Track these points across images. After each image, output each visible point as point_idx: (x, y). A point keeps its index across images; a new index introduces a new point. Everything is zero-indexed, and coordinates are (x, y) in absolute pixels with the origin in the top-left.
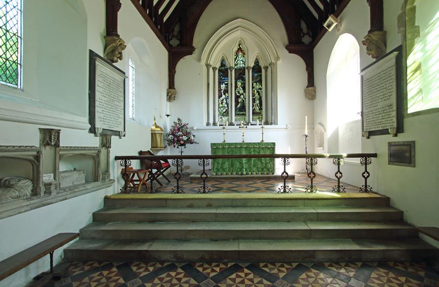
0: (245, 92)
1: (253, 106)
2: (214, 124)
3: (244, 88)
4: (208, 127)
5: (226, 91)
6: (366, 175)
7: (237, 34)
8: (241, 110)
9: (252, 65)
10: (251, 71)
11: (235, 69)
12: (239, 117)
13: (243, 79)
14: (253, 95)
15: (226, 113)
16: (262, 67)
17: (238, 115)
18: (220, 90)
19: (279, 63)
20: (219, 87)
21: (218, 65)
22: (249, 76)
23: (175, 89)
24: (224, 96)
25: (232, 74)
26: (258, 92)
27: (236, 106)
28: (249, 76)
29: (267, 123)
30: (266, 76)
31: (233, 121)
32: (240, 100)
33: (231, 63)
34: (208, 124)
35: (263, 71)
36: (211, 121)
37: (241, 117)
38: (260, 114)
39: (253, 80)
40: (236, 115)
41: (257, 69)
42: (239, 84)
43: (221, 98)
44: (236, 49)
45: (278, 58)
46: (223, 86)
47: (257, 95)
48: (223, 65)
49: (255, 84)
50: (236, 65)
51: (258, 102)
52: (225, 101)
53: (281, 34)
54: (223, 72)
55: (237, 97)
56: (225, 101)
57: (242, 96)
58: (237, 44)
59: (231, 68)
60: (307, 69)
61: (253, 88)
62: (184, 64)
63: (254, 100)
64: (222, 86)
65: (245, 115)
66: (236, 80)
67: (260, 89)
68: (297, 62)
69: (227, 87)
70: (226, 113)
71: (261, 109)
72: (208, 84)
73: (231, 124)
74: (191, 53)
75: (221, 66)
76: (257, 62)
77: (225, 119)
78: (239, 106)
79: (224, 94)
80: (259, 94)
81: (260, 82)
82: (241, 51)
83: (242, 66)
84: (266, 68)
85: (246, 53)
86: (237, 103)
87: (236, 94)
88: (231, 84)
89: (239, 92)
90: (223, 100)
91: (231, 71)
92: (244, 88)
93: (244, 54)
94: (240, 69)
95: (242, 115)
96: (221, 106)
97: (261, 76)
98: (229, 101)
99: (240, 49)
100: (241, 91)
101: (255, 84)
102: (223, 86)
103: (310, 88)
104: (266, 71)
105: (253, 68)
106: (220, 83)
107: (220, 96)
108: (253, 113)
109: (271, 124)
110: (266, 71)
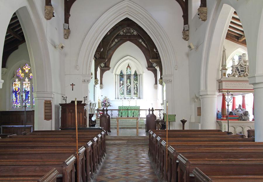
0: (130, 85)
1: (134, 90)
2: (118, 98)
3: (130, 83)
4: (115, 100)
5: (123, 84)
6: (160, 115)
7: (128, 62)
8: (129, 92)
9: (133, 73)
10: (133, 76)
11: (127, 75)
12: (128, 95)
13: (130, 79)
14: (134, 85)
15: (123, 94)
16: (138, 74)
17: (128, 94)
18: (120, 84)
19: (144, 74)
20: (120, 82)
21: (119, 73)
22: (132, 78)
23: (102, 84)
24: (122, 86)
25: (125, 77)
26: (136, 85)
27: (127, 91)
28: (132, 78)
29: (139, 98)
30: (139, 79)
31: (126, 97)
32: (128, 88)
33: (125, 73)
34: (116, 98)
35: (138, 76)
36: (117, 97)
37: (129, 95)
38: (137, 94)
39: (134, 79)
40: (127, 94)
41: (136, 75)
42: (128, 81)
43: (121, 87)
44: (127, 66)
45: (143, 72)
46: (121, 82)
47: (135, 86)
48: (121, 73)
49: (135, 81)
50: (127, 73)
51: (136, 89)
52: (122, 88)
53: (144, 62)
54: (122, 75)
55: (127, 87)
56: (122, 88)
57: (129, 86)
58: (128, 64)
59: (125, 75)
60: (155, 76)
61: (134, 83)
62: (106, 74)
63: (134, 88)
64: (121, 82)
65: (131, 94)
66: (127, 79)
67: (137, 83)
68: (151, 74)
69: (123, 82)
70: (123, 94)
71: (137, 92)
72: (116, 82)
73: (125, 99)
74: (109, 70)
75: (121, 74)
76: (136, 72)
77: (123, 96)
78: (128, 90)
79: (122, 85)
80: (136, 86)
81: (137, 80)
82: (129, 67)
83: (129, 73)
84: (139, 75)
85: (131, 68)
86: (127, 89)
87: (127, 85)
88: (125, 82)
89: (128, 85)
90: (121, 88)
91: (125, 76)
92: (130, 83)
93: (130, 68)
94: (129, 75)
95: (129, 94)
96: (120, 90)
97: (137, 78)
98: (124, 88)
99: (129, 66)
100: (129, 84)
101: (135, 81)
102: (121, 82)
103: (156, 85)
104: (139, 76)
105: (134, 75)
106: (120, 80)
107: (120, 86)
108: (134, 94)
109: (141, 99)
110: (139, 76)
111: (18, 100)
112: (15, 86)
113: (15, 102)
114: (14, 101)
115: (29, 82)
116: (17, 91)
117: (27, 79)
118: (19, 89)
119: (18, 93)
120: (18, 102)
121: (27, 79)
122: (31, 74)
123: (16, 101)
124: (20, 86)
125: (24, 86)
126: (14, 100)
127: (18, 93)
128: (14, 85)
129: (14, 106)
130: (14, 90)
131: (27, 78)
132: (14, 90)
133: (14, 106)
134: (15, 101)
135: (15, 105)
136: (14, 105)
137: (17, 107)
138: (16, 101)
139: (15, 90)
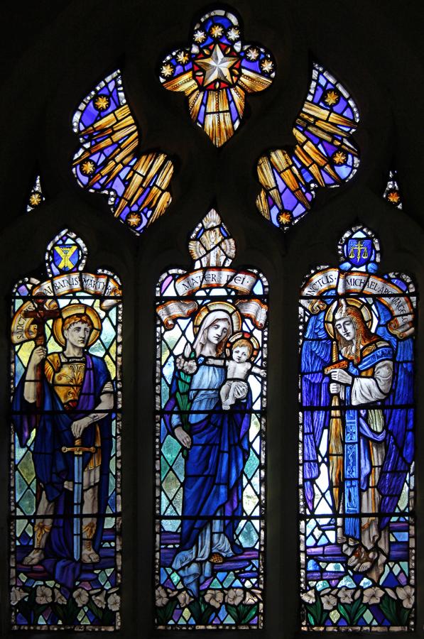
111: (85, 527)
112: (41, 340)
113: (34, 557)
114: (27, 549)
115: (243, 282)
116: (76, 411)
117: (212, 238)
118: (96, 370)
119: (79, 426)
120: (89, 555)
121: (212, 238)
122: (279, 158)
123: (58, 546)
124: (108, 332)
125: (176, 339)
126: (21, 525)
127: (79, 426)
128: (20, 324)
129: (29, 608)
130: (30, 393)
131: (213, 218)
132: (30, 393)
133: (29, 608)
134: (40, 540)
135: (46, 592)
136: (17, 596)
137: (71, 618)
138: (58, 546)
139: (46, 386)
